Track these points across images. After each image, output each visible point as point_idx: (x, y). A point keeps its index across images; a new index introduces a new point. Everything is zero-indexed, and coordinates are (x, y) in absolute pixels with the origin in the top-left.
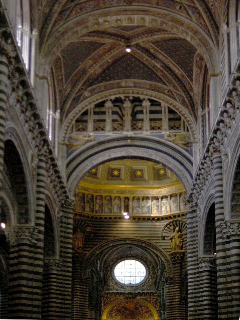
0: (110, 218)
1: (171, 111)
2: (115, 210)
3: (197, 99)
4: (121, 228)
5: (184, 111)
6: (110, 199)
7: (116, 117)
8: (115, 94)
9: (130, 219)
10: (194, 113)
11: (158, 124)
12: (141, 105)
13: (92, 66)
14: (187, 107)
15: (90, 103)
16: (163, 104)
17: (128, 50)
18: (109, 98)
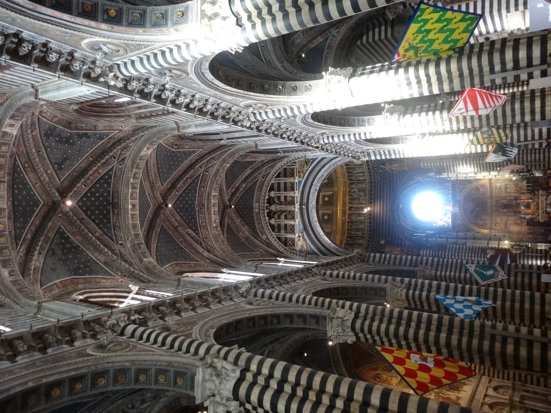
0: (370, 223)
1: (278, 176)
2: (362, 218)
3: (270, 156)
4: (380, 214)
5: (279, 165)
6: (351, 222)
7: (282, 217)
8: (265, 216)
9: (371, 207)
10: (281, 158)
11: (289, 186)
12: (273, 198)
13: (243, 232)
14: (276, 164)
15: (272, 235)
16: (272, 182)
17: (233, 207)
18: (268, 221)
